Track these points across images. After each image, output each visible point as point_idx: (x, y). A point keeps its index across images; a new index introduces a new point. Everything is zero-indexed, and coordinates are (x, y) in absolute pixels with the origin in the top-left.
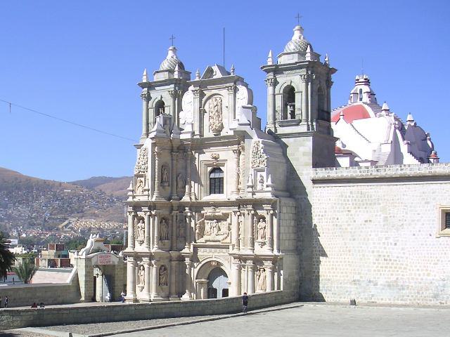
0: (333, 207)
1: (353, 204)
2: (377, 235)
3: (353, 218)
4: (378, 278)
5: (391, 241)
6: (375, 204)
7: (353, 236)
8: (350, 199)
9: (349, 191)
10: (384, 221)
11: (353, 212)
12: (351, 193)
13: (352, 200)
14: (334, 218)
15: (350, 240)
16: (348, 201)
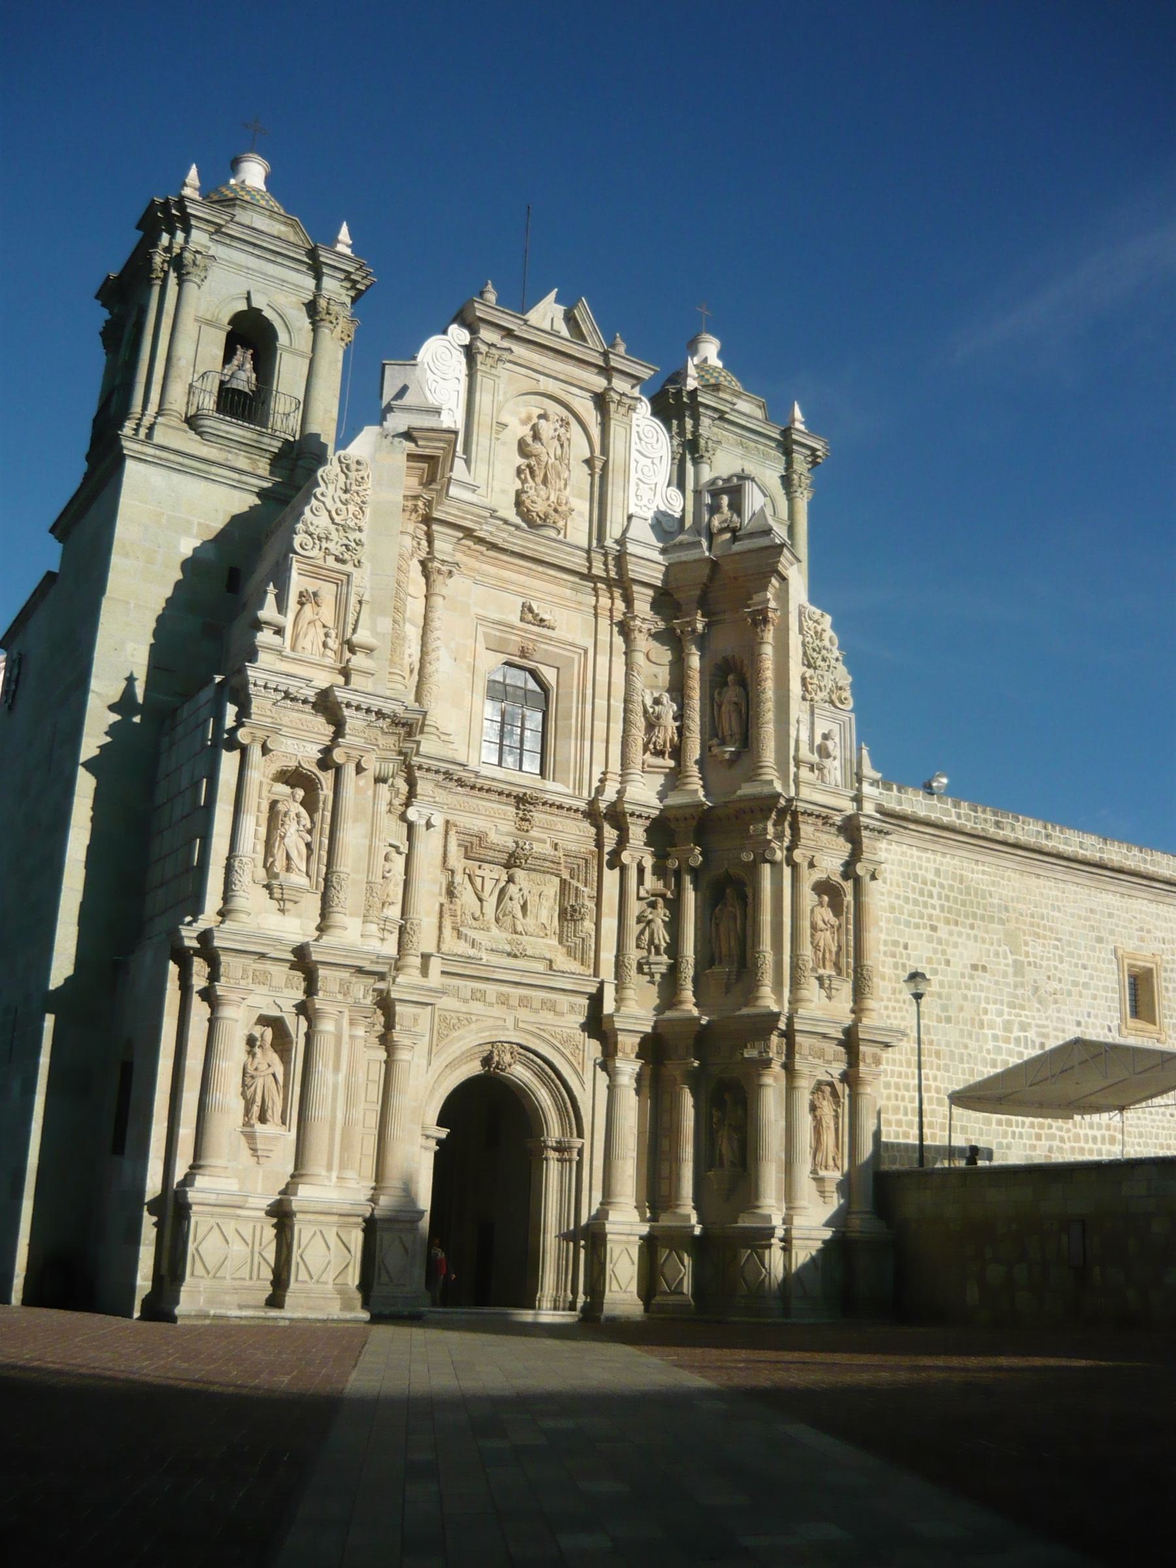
0: (892, 909)
1: (942, 907)
2: (1000, 1013)
3: (944, 952)
4: (1008, 1147)
5: (1031, 1034)
6: (992, 919)
7: (944, 1008)
8: (935, 891)
9: (932, 866)
10: (1015, 974)
11: (942, 933)
12: (938, 872)
13: (939, 895)
14: (896, 943)
15: (939, 1020)
16: (931, 896)
